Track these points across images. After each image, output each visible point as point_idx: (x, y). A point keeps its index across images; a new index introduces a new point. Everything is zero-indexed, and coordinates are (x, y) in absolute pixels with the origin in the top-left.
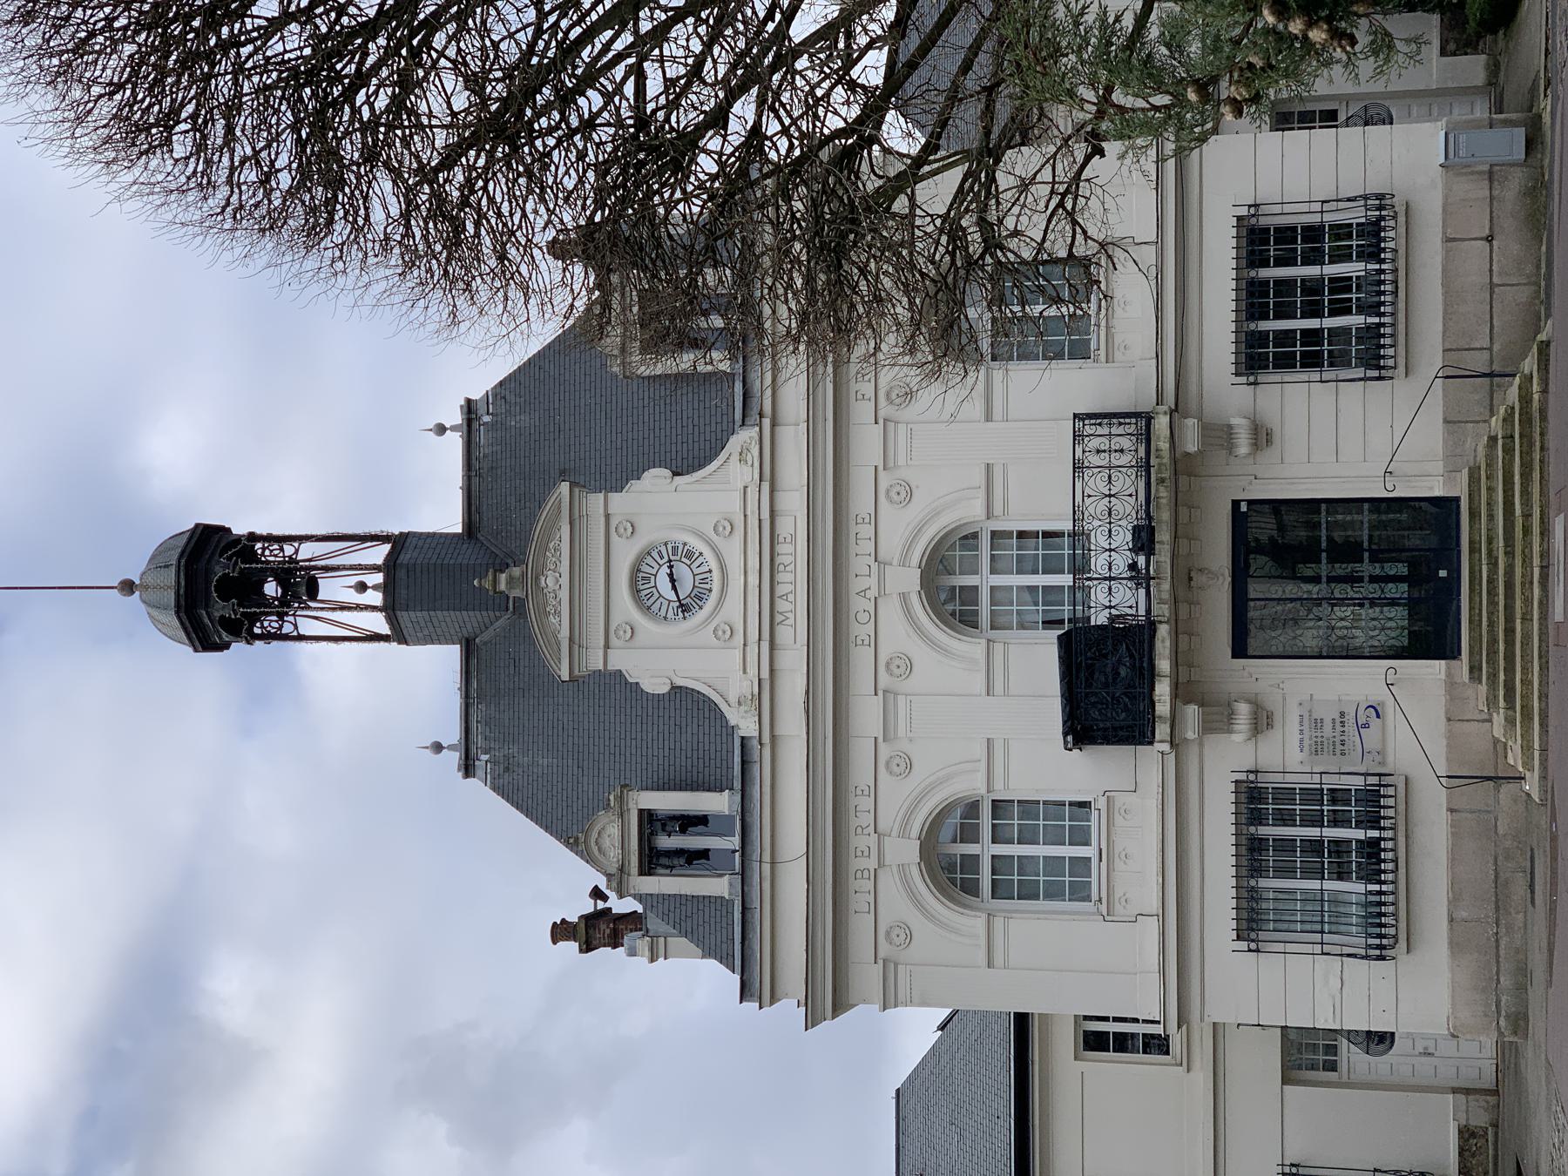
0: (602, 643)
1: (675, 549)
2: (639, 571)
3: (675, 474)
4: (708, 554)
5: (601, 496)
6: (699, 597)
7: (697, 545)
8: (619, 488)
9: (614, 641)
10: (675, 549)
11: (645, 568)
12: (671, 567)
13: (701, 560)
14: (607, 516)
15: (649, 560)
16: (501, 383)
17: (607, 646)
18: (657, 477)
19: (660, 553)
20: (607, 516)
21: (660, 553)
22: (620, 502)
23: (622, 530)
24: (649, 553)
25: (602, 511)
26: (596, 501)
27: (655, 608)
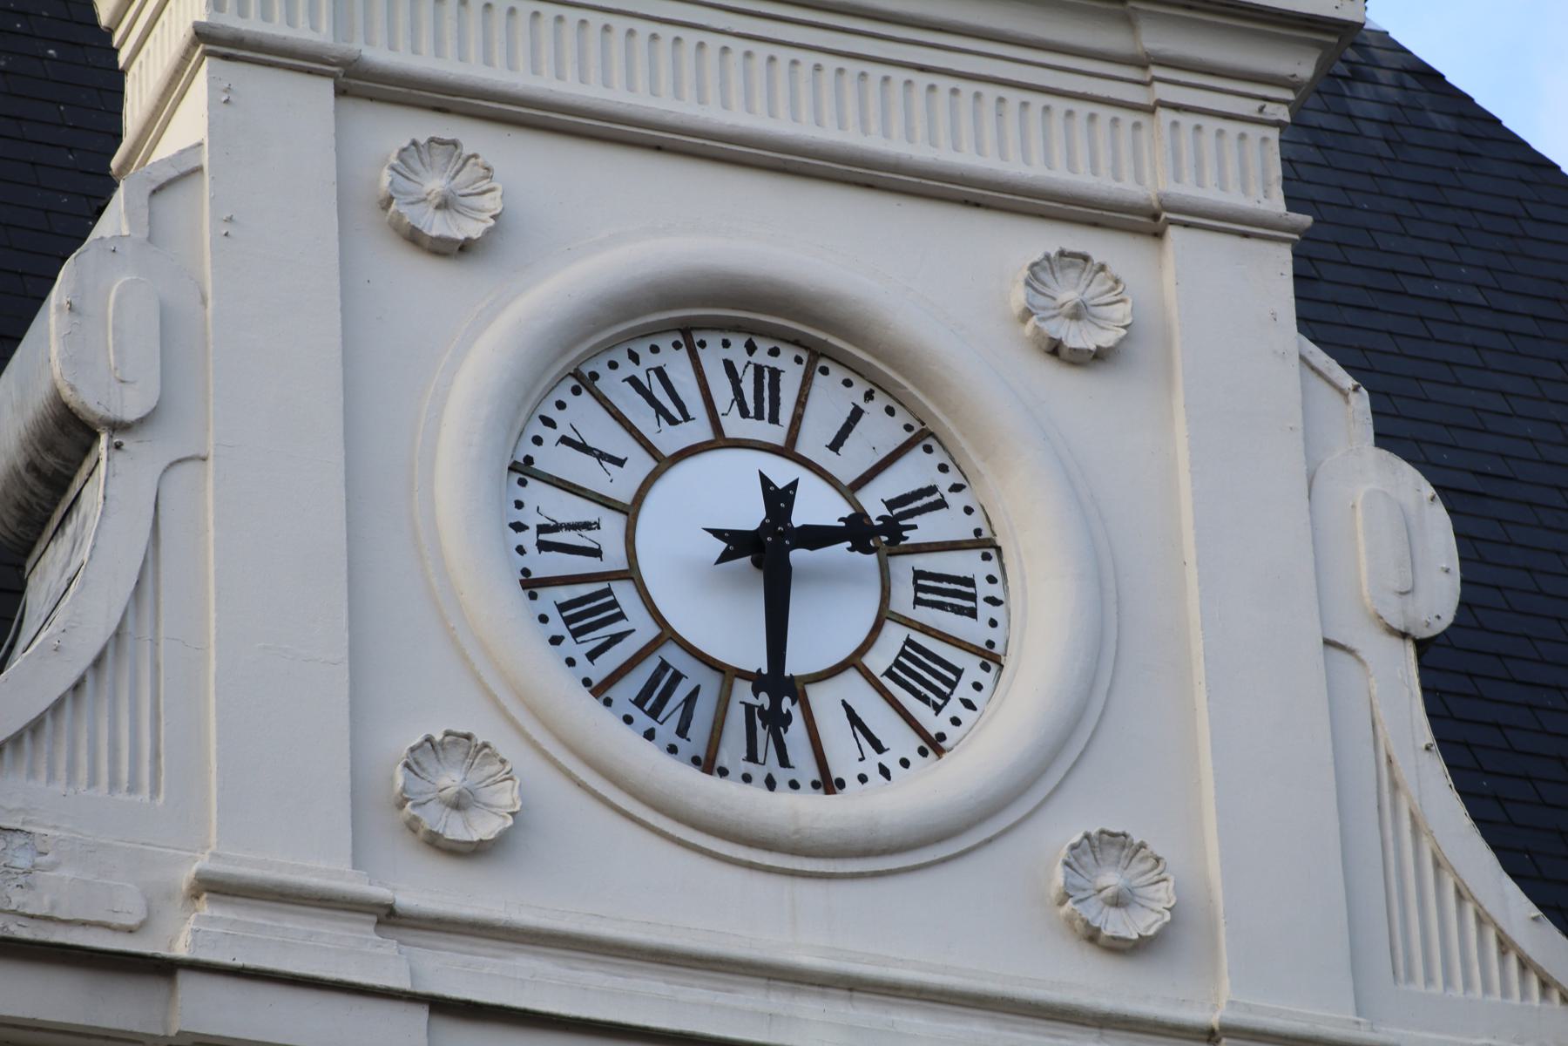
0: (379, 55)
1: (956, 594)
2: (816, 357)
3: (1422, 646)
4: (923, 791)
5: (1275, 204)
6: (659, 685)
7: (995, 733)
8: (1339, 306)
9: (392, 131)
10: (956, 594)
11: (831, 400)
12: (857, 532)
13: (900, 741)
14: (1148, 222)
15: (880, 431)
16: (1430, 78)
17: (357, 83)
18: (1397, 543)
19: (926, 500)
20: (1148, 222)
21: (926, 500)
22: (1233, 306)
23: (1068, 292)
24: (921, 437)
25: (1187, 190)
26: (1241, 166)
27: (584, 417)
